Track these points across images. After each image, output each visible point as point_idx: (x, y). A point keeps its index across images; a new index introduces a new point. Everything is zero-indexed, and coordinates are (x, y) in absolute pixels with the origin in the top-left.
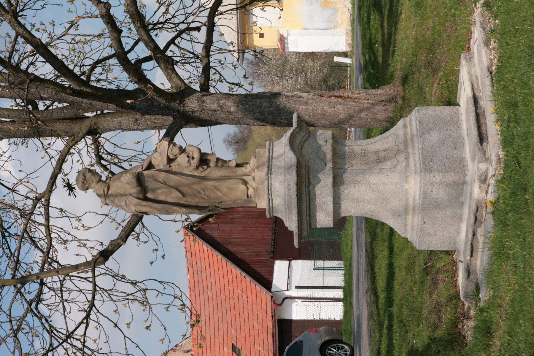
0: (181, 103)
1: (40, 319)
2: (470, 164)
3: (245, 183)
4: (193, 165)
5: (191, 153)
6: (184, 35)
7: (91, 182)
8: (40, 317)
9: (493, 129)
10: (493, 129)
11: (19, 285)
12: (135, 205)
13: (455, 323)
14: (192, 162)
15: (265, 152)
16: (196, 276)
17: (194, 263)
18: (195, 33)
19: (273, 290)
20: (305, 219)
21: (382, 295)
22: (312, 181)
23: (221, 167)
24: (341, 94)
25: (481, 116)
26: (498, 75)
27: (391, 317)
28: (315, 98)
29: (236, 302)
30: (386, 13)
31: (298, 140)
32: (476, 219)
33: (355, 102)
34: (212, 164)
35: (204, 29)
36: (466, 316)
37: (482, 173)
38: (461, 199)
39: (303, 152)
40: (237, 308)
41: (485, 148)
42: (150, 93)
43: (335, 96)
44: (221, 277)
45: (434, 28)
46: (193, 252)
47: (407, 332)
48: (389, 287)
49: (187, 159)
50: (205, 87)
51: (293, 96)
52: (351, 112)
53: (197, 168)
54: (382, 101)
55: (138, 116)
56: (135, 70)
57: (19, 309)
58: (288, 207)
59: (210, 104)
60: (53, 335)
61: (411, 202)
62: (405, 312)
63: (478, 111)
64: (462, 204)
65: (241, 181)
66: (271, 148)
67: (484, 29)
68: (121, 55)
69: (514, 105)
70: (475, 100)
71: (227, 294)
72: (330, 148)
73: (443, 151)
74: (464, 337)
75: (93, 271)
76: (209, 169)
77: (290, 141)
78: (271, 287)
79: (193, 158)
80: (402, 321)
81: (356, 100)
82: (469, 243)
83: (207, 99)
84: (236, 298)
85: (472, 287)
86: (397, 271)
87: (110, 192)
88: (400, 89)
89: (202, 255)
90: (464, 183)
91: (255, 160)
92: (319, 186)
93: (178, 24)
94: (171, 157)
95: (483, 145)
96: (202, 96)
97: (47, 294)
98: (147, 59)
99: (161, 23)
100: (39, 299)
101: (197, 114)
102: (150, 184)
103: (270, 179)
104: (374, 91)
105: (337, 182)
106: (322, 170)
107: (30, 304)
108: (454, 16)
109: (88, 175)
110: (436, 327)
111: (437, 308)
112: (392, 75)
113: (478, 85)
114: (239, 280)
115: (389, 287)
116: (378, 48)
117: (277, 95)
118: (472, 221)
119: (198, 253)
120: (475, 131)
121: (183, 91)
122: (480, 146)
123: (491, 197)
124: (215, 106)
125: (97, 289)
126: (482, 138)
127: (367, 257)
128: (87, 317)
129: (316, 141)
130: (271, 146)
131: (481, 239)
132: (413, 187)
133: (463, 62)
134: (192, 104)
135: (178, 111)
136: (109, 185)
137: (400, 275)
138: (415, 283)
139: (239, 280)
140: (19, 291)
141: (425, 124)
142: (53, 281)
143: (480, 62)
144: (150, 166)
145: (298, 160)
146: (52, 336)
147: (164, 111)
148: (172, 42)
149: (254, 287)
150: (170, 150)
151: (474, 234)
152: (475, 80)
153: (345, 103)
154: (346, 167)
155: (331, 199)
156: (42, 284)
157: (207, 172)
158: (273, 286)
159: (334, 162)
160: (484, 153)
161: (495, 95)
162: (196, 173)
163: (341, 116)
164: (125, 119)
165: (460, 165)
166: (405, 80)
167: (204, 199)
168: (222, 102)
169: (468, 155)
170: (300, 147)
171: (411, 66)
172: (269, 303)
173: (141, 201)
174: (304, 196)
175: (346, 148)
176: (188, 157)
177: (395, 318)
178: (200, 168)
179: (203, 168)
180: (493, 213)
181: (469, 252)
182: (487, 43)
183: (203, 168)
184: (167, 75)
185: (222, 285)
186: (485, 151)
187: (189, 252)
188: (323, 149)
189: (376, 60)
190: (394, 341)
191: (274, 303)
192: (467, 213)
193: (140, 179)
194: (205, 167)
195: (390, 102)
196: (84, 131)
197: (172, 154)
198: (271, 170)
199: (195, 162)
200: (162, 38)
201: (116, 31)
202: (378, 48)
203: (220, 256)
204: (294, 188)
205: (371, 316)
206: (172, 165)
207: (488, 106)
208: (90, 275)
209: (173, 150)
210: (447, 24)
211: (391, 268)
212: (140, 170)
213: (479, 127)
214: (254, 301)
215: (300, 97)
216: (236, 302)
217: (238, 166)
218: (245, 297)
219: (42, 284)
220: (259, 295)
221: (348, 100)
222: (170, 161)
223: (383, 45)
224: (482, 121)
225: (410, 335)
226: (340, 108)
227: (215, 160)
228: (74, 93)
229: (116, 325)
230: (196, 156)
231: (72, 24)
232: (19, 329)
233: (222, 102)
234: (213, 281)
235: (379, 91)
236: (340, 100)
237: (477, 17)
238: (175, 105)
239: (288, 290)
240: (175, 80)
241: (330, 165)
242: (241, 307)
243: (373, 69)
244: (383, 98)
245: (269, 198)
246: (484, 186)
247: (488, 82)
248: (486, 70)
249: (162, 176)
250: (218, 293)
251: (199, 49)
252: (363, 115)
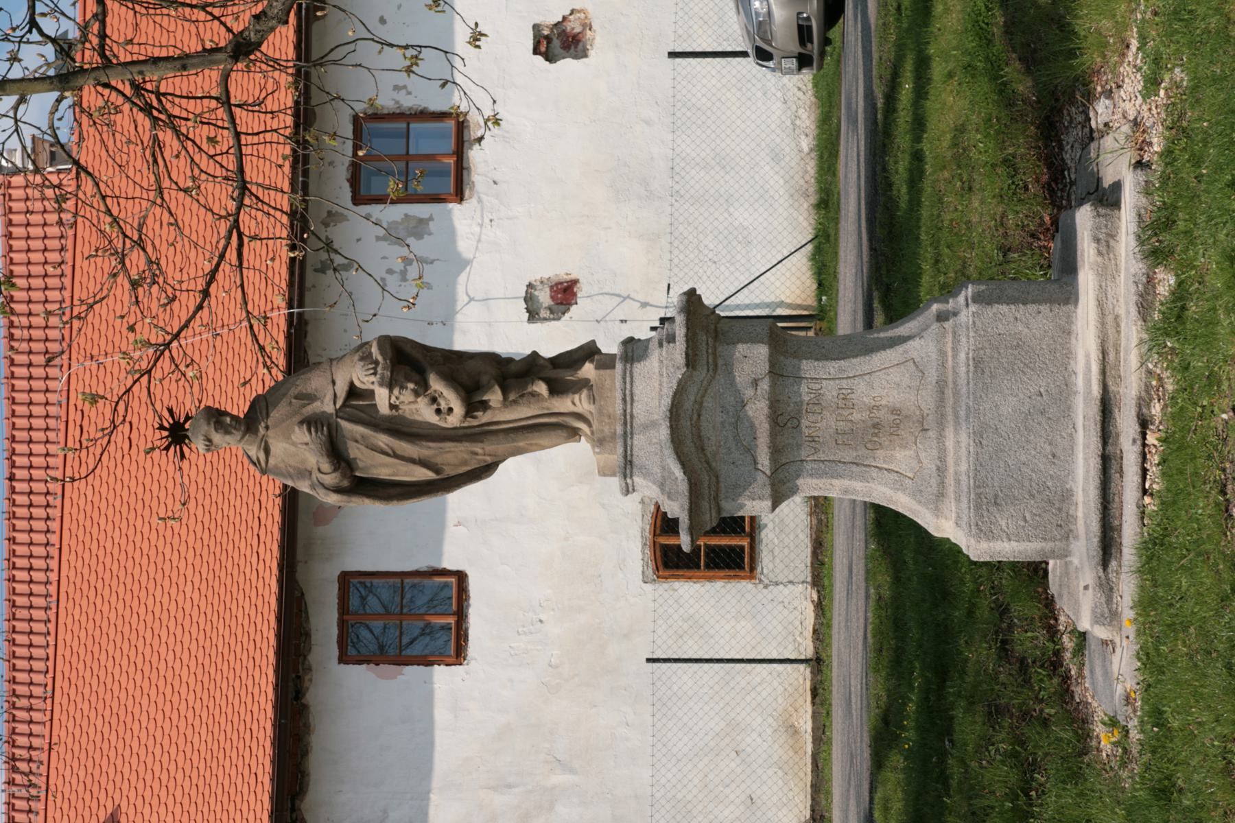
14: (450, 418)
15: (613, 380)
23: (515, 402)
25: (1114, 466)
39: (704, 424)
41: (1112, 576)
66: (628, 386)
72: (766, 411)
73: (1024, 469)
77: (671, 411)
79: (450, 410)
87: (272, 461)
95: (1110, 570)
120: (1095, 526)
122: (1101, 573)
129: (732, 382)
130: (628, 379)
136: (266, 443)
152: (1111, 332)
154: (803, 454)
170: (695, 417)
175: (804, 388)
186: (1111, 589)
194: (479, 414)
198: (631, 462)
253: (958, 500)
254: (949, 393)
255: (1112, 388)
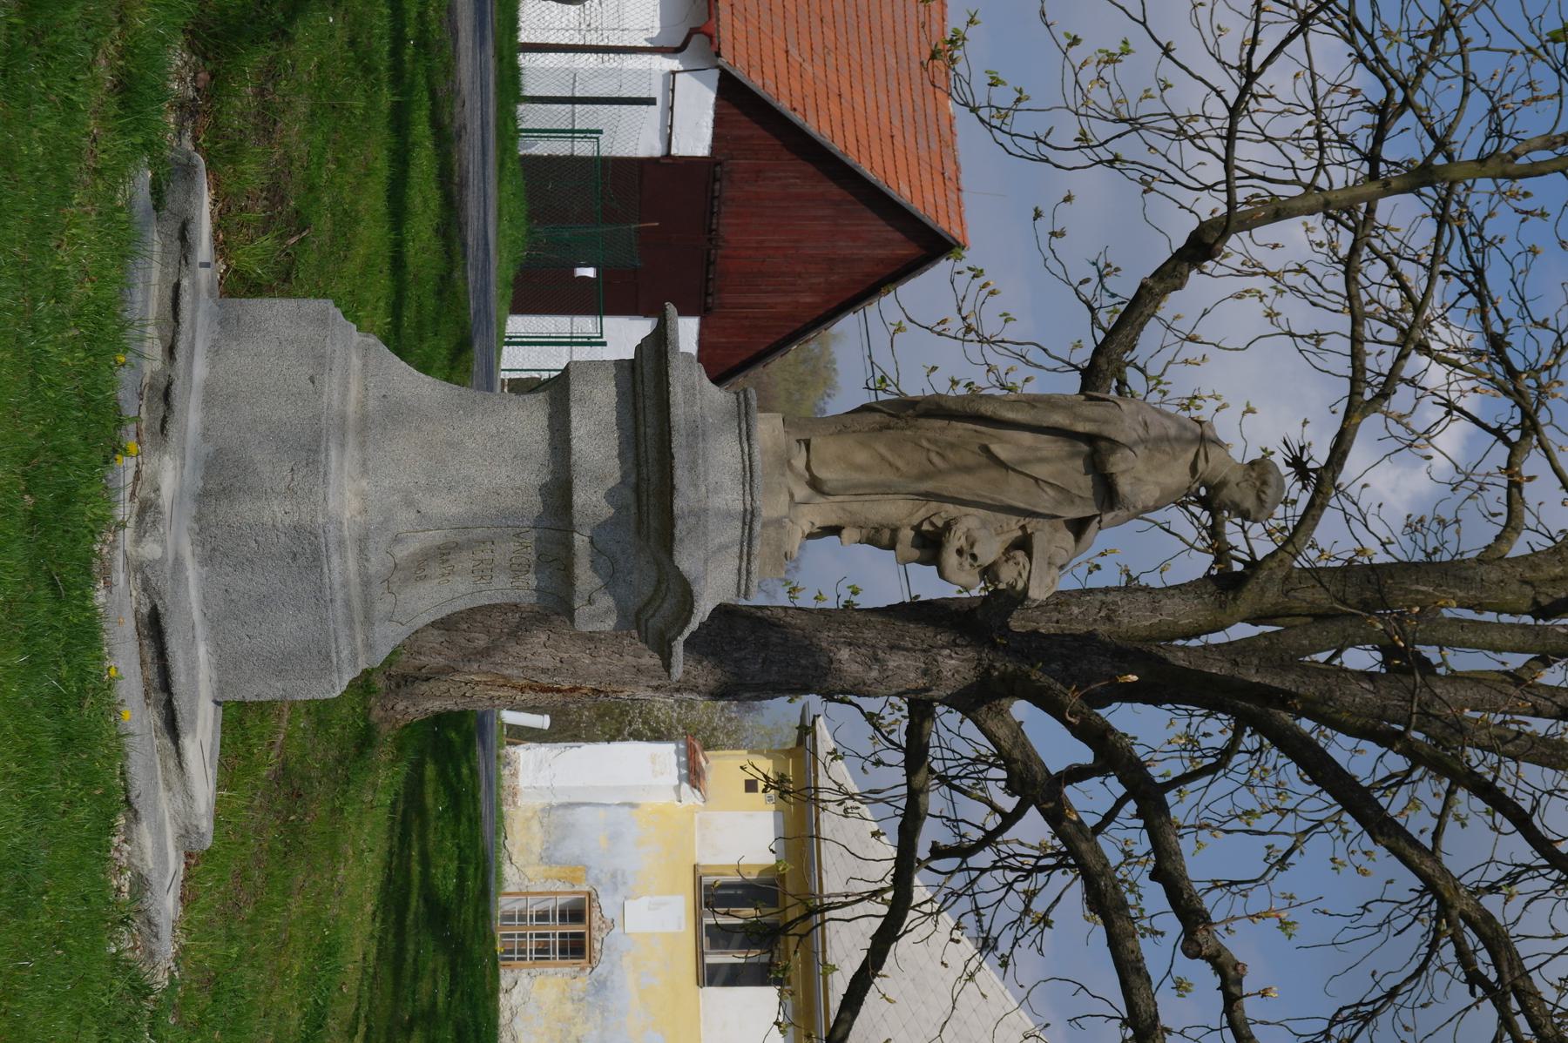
0: (987, 671)
1: (1381, 60)
2: (187, 550)
3: (815, 484)
4: (959, 533)
5: (967, 567)
6: (977, 835)
7: (1243, 485)
8: (1378, 66)
9: (124, 660)
10: (124, 660)
11: (1440, 160)
12: (1124, 423)
13: (215, 88)
16: (930, 111)
17: (935, 146)
18: (947, 838)
19: (714, 74)
20: (649, 388)
21: (421, 129)
22: (629, 495)
23: (883, 526)
24: (542, 696)
25: (156, 683)
26: (114, 805)
27: (398, 76)
28: (615, 687)
29: (817, 39)
30: (415, 902)
31: (668, 606)
32: (167, 395)
33: (504, 677)
34: (907, 535)
35: (923, 852)
36: (187, 109)
37: (155, 527)
38: (209, 448)
40: (815, 21)
41: (145, 600)
42: (1073, 699)
43: (559, 691)
44: (860, 108)
45: (286, 893)
46: (938, 179)
47: (352, 43)
48: (401, 159)
49: (976, 551)
50: (921, 711)
51: (678, 690)
52: (514, 648)
53: (948, 526)
54: (428, 679)
55: (1102, 629)
56: (1112, 756)
57: (1439, 93)
58: (697, 432)
59: (906, 667)
60: (1346, 18)
61: (352, 451)
62: (359, 104)
63: (164, 697)
64: (206, 435)
65: (826, 489)
67: (150, 922)
68: (1148, 796)
69: (67, 742)
70: (172, 726)
71: (843, 61)
72: (578, 583)
74: (191, 47)
75: (1231, 203)
76: (915, 522)
77: (692, 606)
78: (720, 80)
79: (960, 552)
80: (368, 70)
81: (501, 681)
82: (185, 326)
83: (914, 680)
84: (818, 48)
85: (173, 200)
86: (381, 206)
88: (377, 714)
89: (914, 171)
90: (203, 496)
91: (788, 548)
92: (611, 483)
93: (994, 867)
94: (1020, 555)
95: (149, 606)
96: (927, 690)
97: (1358, 124)
98: (1077, 774)
99: (1042, 869)
100: (1384, 115)
101: (942, 639)
102: (1084, 484)
103: (748, 498)
104: (450, 705)
105: (559, 492)
106: (602, 526)
107: (1407, 102)
108: (231, 938)
109: (1249, 503)
110: (271, 73)
111: (267, 120)
112: (400, 749)
113: (165, 767)
114: (810, 101)
115: (401, 159)
116: (434, 801)
117: (717, 694)
118: (177, 389)
119: (926, 176)
120: (174, 644)
121: (980, 702)
122: (159, 603)
123: (125, 467)
124: (895, 661)
125: (1218, 146)
126: (154, 627)
127: (461, 227)
128: (1251, 77)
129: (618, 602)
131: (154, 349)
132: (347, 495)
133: (206, 825)
134: (956, 666)
135: (994, 647)
137: (373, 201)
138: (331, 182)
139: (810, 101)
140: (1441, 145)
141: (315, 653)
142: (1342, 175)
143: (159, 831)
144: (1079, 527)
145: (670, 552)
146: (1348, 14)
147: (1035, 646)
148: (1009, 819)
149: (767, 81)
150: (1025, 575)
151: (171, 351)
152: (174, 778)
153: (530, 673)
154: (534, 533)
155: (576, 444)
156: (1373, 158)
157: (922, 513)
158: (716, 84)
159: (568, 546)
160: (146, 587)
161: (119, 753)
162: (951, 510)
163: (544, 637)
164: (1137, 619)
165: (215, 549)
166: (365, 739)
167: (929, 440)
168: (874, 674)
169: (192, 571)
170: (664, 587)
171: (348, 782)
172: (725, 34)
173: (1106, 434)
174: (653, 454)
175: (534, 583)
176: (974, 557)
177: (385, 76)
178: (940, 523)
179: (932, 524)
180: (120, 423)
181: (186, 299)
182: (141, 883)
183: (932, 524)
184: (1025, 745)
185: (857, 86)
186: (145, 590)
187: (950, 180)
188: (598, 582)
189: (446, 773)
190: (386, 11)
191: (711, 37)
192: (191, 416)
193: (1108, 494)
194: (926, 527)
195: (405, 677)
196: (1252, 586)
197: (1017, 564)
199: (956, 540)
200: (1033, 829)
201: (1167, 874)
202: (434, 801)
203: (865, 169)
204: (681, 475)
205: (450, 69)
206: (1020, 533)
207: (137, 717)
208: (1241, 195)
209: (1015, 574)
210: (249, 911)
211: (398, 211)
212: (1107, 517)
213: (161, 654)
214: (766, 42)
215: (657, 689)
216: (817, 39)
217: (835, 530)
218: (793, 52)
219: (1373, 158)
220: (755, 60)
221: (523, 682)
222: (1024, 544)
223: (422, 811)
224: (152, 672)
225: (342, 36)
226: (545, 660)
227: (898, 547)
228: (1282, 699)
229: (1167, 51)
230: (951, 559)
231: (1282, 863)
232: (1438, 33)
233: (874, 674)
234: (882, 98)
235: (435, 706)
236: (545, 680)
237: (167, 948)
238: (1003, 665)
239: (674, 73)
240: (1002, 732)
241: (580, 541)
242: (803, 23)
243: (450, 742)
244: (424, 687)
245: (750, 446)
246: (145, 492)
247: (139, 782)
248: (142, 812)
249: (1045, 501)
250: (867, 63)
251: (936, 800)
252: (482, 641)
253: (341, 543)
254: (358, 617)
255: (168, 742)
